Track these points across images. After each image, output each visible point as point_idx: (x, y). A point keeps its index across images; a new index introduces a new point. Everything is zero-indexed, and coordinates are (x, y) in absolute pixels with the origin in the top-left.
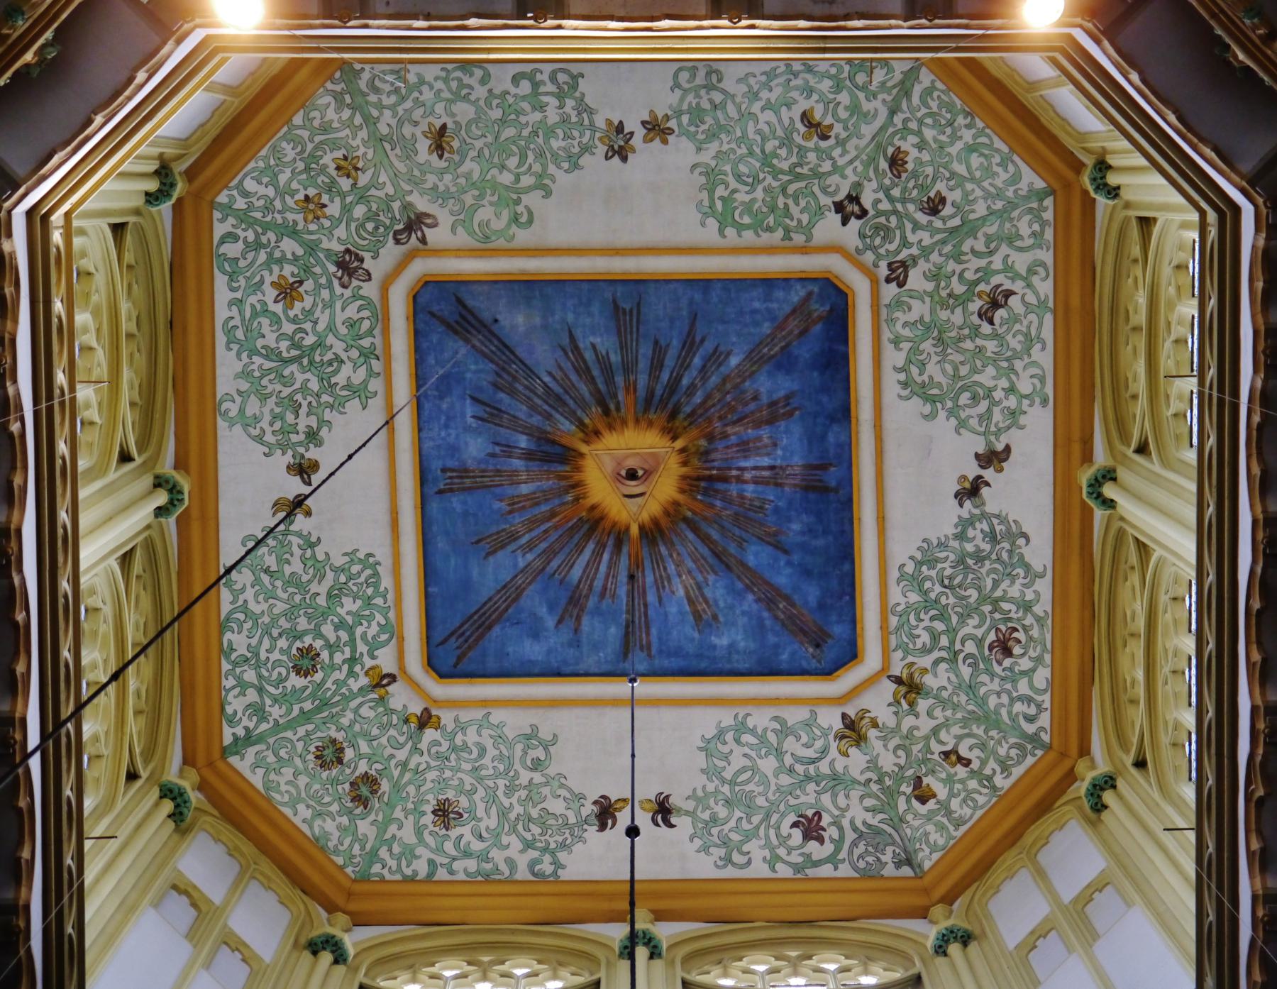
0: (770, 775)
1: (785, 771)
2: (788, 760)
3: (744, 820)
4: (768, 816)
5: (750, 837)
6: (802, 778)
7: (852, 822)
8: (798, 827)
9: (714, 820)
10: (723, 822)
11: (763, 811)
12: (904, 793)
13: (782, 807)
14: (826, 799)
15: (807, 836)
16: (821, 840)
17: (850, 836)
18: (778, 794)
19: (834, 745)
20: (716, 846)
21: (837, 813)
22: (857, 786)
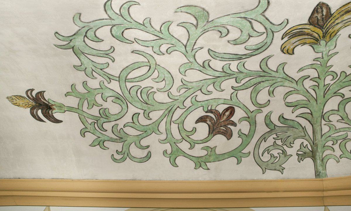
0: (175, 72)
1: (196, 66)
2: (202, 56)
3: (141, 117)
4: (170, 111)
5: (149, 132)
6: (217, 74)
7: (268, 117)
8: (205, 121)
9: (105, 114)
10: (116, 117)
11: (165, 107)
12: (343, 96)
13: (188, 103)
14: (244, 96)
15: (213, 131)
16: (228, 135)
17: (262, 129)
18: (183, 90)
19: (278, 42)
20: (112, 140)
21: (252, 108)
22: (287, 83)
